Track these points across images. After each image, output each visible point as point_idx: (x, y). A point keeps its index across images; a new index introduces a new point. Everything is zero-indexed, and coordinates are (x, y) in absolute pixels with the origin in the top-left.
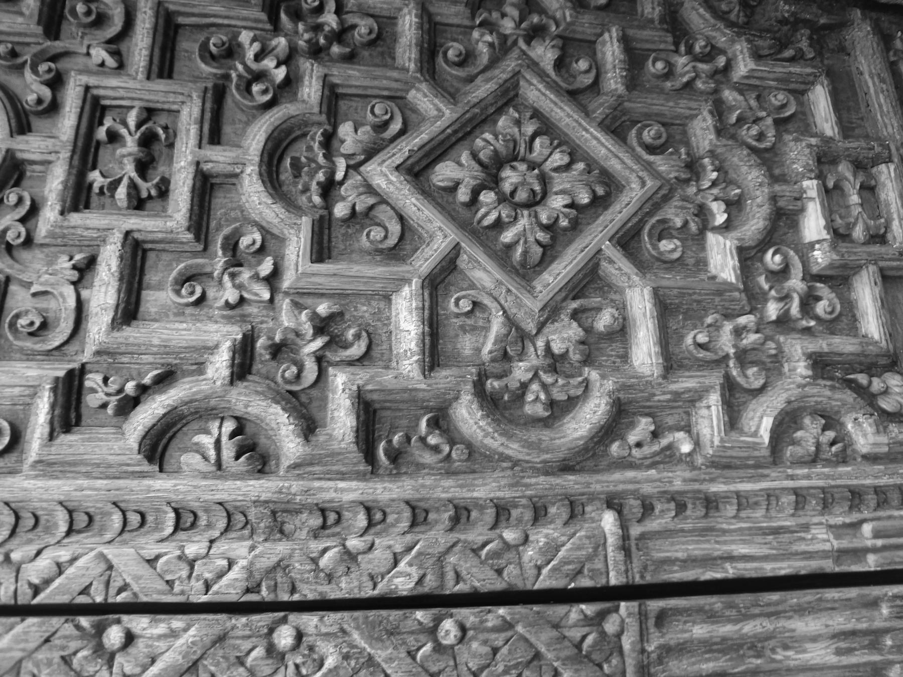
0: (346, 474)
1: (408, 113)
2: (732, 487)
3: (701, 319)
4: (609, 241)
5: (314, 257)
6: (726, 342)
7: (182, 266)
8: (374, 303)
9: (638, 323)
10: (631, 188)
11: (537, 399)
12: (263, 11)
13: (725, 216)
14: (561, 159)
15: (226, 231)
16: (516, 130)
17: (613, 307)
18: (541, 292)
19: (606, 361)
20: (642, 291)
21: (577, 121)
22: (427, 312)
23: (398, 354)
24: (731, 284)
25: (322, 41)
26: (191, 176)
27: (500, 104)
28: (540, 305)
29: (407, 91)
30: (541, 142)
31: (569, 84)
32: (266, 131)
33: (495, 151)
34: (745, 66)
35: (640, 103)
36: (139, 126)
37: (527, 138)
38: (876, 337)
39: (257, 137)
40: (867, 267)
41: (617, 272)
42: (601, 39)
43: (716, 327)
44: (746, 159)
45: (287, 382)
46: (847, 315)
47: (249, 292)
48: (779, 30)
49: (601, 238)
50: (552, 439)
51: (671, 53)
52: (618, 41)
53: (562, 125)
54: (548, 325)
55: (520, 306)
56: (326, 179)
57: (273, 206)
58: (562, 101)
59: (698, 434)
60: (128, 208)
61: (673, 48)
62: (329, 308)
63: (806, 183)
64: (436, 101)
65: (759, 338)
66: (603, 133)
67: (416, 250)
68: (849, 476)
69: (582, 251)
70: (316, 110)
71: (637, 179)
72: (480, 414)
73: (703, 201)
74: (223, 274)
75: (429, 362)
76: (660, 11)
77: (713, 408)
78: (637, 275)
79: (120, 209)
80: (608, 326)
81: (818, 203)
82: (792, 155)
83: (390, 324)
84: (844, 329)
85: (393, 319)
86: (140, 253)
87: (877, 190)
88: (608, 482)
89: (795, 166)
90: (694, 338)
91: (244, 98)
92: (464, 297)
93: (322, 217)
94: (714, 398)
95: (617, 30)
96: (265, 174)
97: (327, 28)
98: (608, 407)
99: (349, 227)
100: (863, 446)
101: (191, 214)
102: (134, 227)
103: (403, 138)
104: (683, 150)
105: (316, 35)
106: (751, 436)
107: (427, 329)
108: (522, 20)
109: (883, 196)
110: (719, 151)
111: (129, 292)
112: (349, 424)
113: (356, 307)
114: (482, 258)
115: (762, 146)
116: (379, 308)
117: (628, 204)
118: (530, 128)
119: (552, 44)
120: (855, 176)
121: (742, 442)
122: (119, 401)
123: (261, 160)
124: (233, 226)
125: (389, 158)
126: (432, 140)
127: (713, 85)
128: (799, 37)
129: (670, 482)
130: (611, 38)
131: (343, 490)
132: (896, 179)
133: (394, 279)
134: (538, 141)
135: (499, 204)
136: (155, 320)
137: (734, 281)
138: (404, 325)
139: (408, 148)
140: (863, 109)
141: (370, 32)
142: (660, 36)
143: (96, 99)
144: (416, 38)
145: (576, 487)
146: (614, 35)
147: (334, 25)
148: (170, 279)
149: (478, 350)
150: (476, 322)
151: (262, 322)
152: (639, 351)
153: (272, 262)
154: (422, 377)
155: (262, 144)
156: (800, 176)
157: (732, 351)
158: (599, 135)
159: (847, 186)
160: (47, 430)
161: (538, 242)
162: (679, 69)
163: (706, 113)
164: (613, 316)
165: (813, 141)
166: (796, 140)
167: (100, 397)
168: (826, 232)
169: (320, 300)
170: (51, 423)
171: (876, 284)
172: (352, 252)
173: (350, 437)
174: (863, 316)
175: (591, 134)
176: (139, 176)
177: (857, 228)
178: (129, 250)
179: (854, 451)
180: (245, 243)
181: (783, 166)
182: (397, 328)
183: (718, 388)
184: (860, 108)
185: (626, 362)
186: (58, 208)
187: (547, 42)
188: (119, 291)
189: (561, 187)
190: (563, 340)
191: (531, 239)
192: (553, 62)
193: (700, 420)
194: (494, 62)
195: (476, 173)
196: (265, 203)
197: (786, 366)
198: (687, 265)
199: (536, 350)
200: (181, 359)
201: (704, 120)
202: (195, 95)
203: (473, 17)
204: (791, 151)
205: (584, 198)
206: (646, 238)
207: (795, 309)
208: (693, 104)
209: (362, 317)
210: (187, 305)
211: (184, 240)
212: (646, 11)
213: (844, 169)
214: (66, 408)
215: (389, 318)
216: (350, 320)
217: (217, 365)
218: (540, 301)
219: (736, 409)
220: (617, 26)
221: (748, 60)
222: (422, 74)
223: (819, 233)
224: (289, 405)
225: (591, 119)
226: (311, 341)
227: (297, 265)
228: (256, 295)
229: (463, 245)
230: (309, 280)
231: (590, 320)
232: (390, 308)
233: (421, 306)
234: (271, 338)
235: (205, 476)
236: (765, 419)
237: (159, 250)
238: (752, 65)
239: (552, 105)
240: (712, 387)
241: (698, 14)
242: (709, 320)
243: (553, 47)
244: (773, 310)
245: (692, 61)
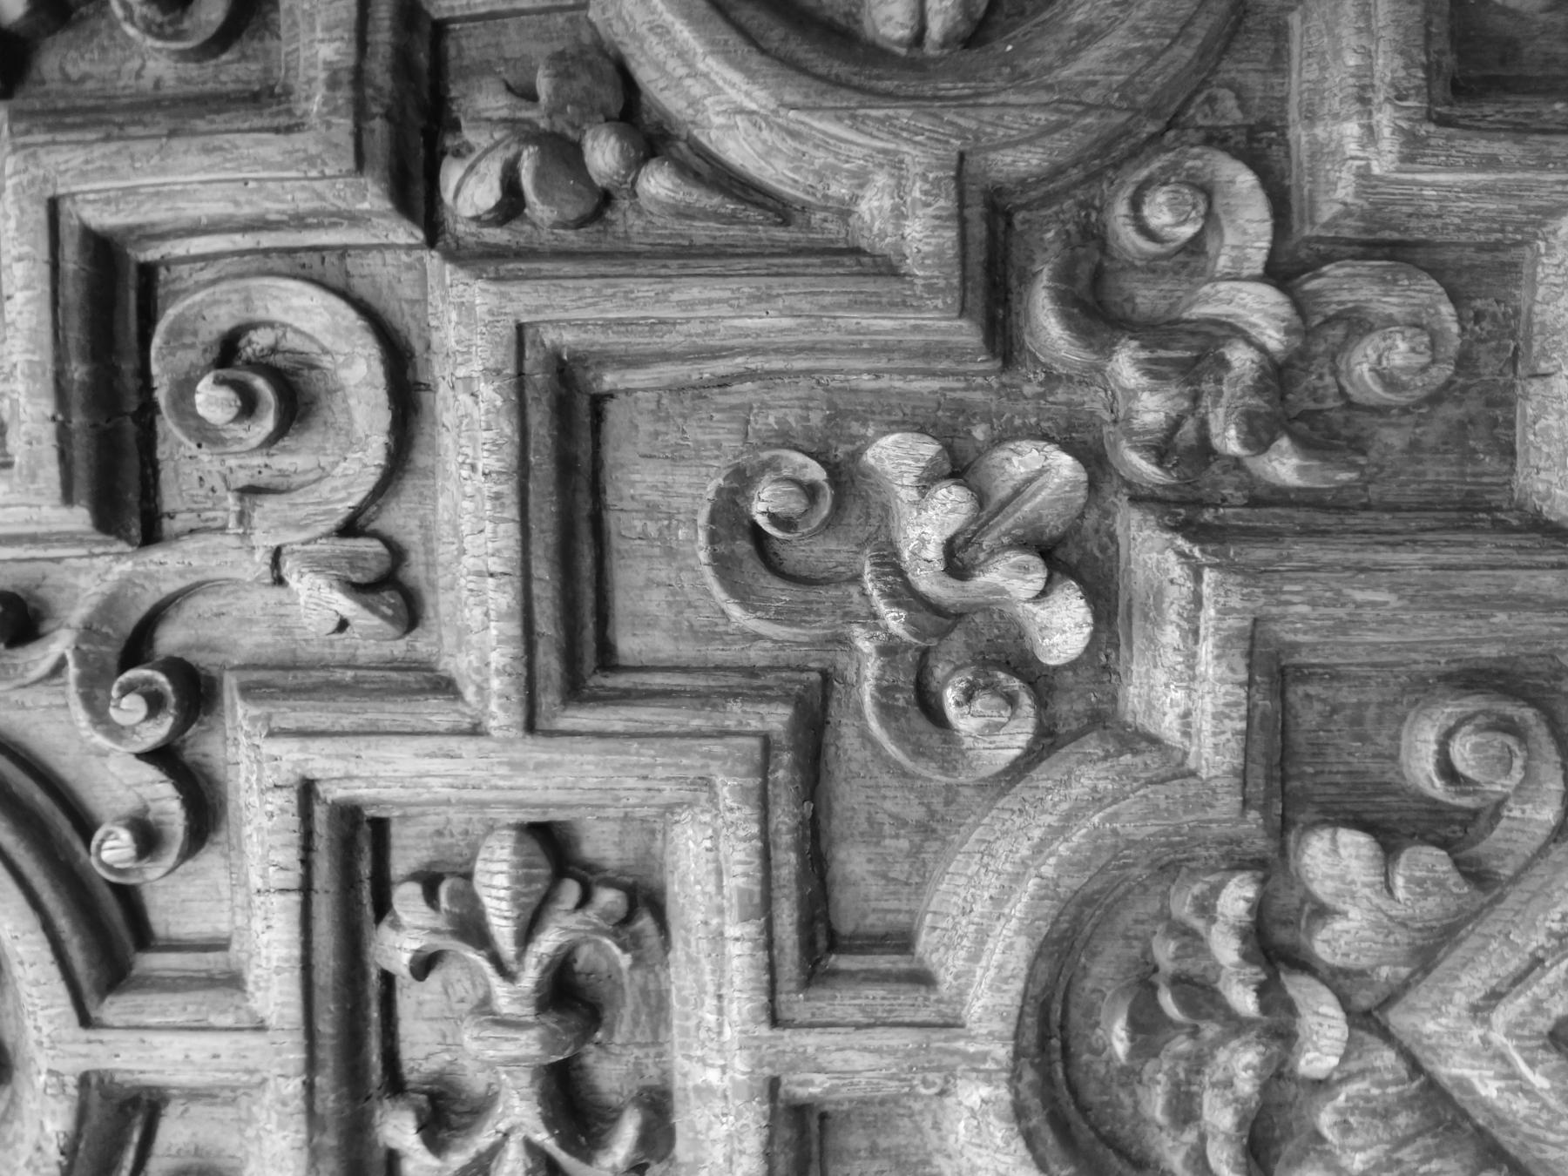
12: (963, 312)
25: (1230, 441)
26: (753, 1142)
32: (1026, 929)
36: (527, 933)
70: (1228, 803)
91: (918, 752)
97: (1241, 357)
105: (1196, 398)
125: (1520, 979)
143: (349, 816)
147: (1274, 339)
176: (564, 1145)
202: (726, 788)
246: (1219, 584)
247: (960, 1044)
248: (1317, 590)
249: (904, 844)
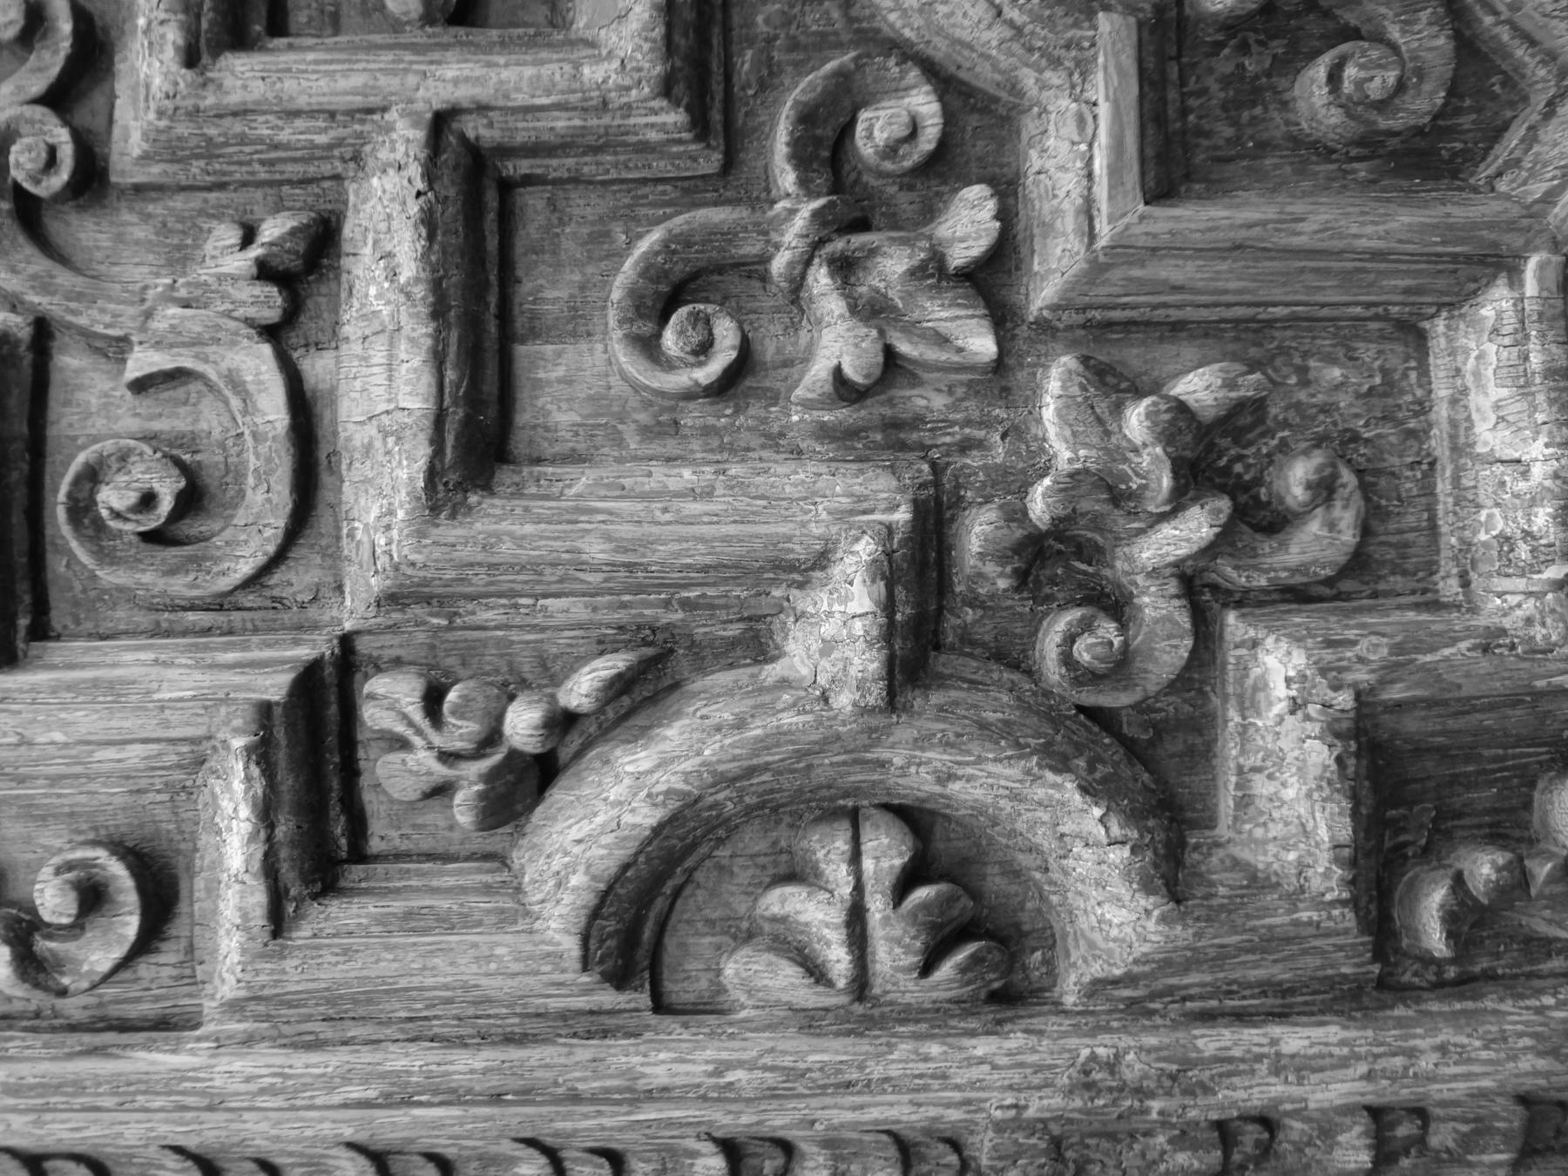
0: (1291, 991)
7: (655, 236)
8: (1367, 351)
15: (800, 90)
23: (1467, 545)
45: (1081, 676)
47: (911, 329)
60: (428, 19)
62: (1230, 384)
67: (1497, 133)
74: (808, 263)
79: (396, 26)
85: (1442, 412)
86: (491, 199)
99: (1244, 48)
101: (669, 26)
102: (463, 94)
111: (472, 356)
112: (1323, 834)
113: (1303, 371)
116: (1384, 372)
122: (491, 777)
124: (830, 66)
131: (1303, 1067)
133: (1455, 257)
136: (574, 458)
148: (616, 295)
151: (965, 447)
153: (991, 205)
160: (258, 898)
167: (423, 762)
169: (1169, 349)
170: (270, 870)
172: (1264, 147)
178: (452, 192)
180: (881, 137)
182: (1461, 448)
186: (173, 36)
188: (438, 359)
200: (686, 604)
209: (1325, 409)
210: (689, 395)
211: (653, 136)
214: (313, 811)
216: (1286, 424)
217: (828, 629)
226: (1163, 517)
227: (1088, 210)
228: (942, 340)
230: (1136, 272)
232: (1424, 371)
235: (809, 1022)
237: (556, 182)
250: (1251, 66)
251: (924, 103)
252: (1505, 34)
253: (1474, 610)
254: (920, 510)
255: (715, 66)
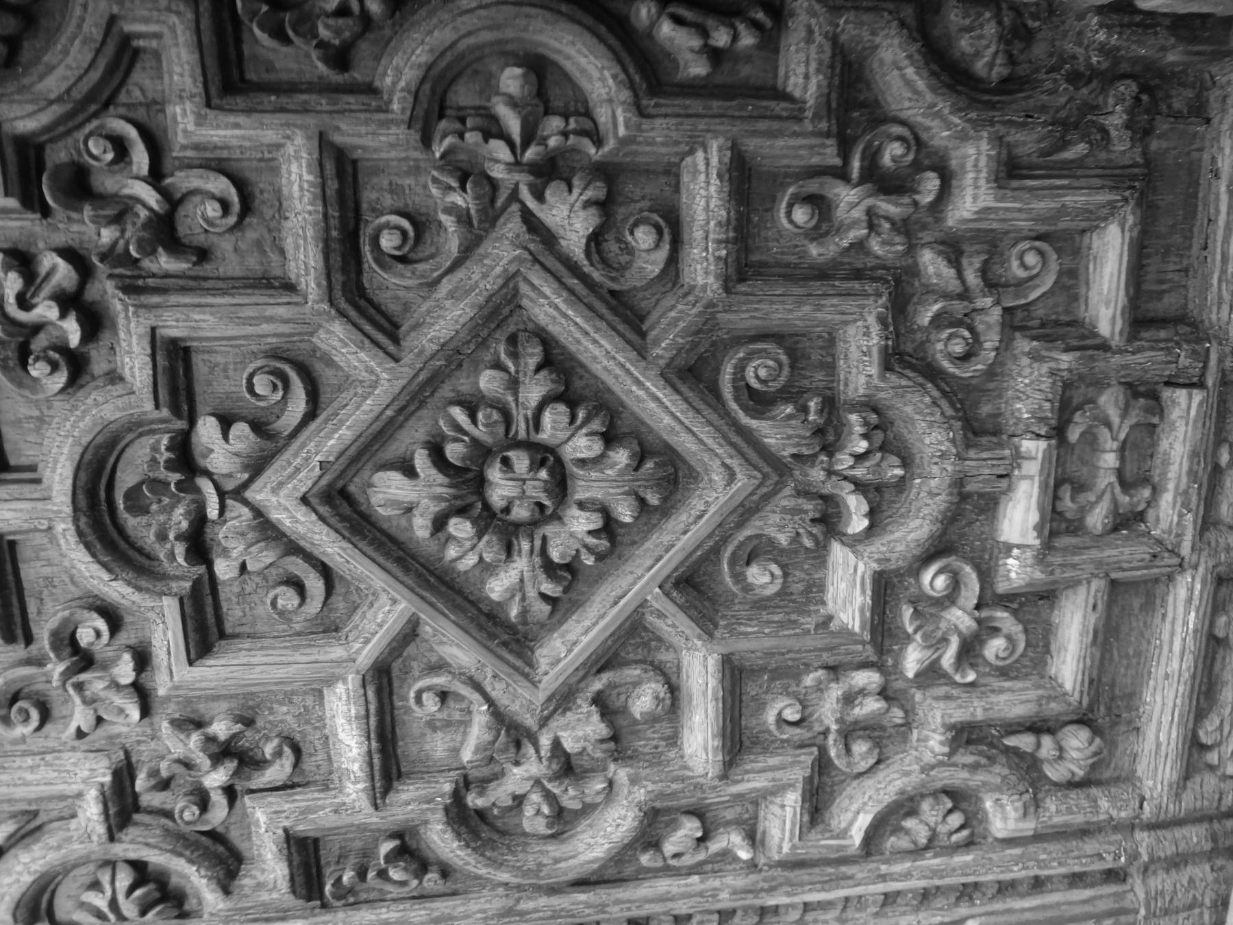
0: (289, 910)
1: (319, 368)
2: (797, 899)
3: (797, 677)
4: (660, 587)
5: (193, 656)
6: (828, 711)
9: (695, 702)
10: (710, 480)
11: (538, 812)
13: (866, 523)
14: (589, 448)
16: (510, 399)
17: (658, 682)
18: (546, 673)
19: (645, 746)
20: (705, 658)
21: (622, 366)
22: (373, 721)
23: (340, 768)
24: (851, 633)
27: (484, 333)
28: (542, 696)
29: (312, 334)
30: (554, 421)
31: (613, 279)
32: (70, 459)
33: (475, 442)
34: (975, 198)
35: (747, 311)
37: (529, 413)
38: (1068, 686)
39: (59, 471)
40: (1089, 583)
41: (670, 629)
42: (689, 160)
43: (819, 688)
44: (928, 411)
46: (1037, 646)
48: (1071, 99)
49: (647, 583)
50: (557, 861)
51: (829, 180)
52: (720, 176)
53: (596, 368)
54: (556, 716)
55: (515, 696)
56: (191, 523)
57: (114, 584)
58: (597, 330)
59: (764, 833)
61: (837, 161)
63: (1028, 445)
64: (363, 355)
65: (879, 709)
66: (668, 390)
68: (964, 869)
69: (616, 603)
70: (149, 406)
71: (722, 470)
72: (456, 844)
73: (835, 491)
75: (382, 786)
76: (819, 86)
77: (788, 809)
78: (699, 638)
80: (647, 713)
81: (1036, 485)
82: (1022, 382)
83: (324, 726)
84: (1025, 666)
85: (328, 721)
87: (1158, 430)
88: (629, 901)
89: (1018, 406)
90: (780, 714)
92: (429, 689)
93: (197, 584)
94: (793, 798)
95: (720, 149)
96: (87, 530)
98: (636, 823)
100: (999, 830)
103: (313, 426)
104: (813, 405)
105: (123, 231)
106: (837, 837)
107: (374, 744)
108: (529, 136)
109: (1164, 445)
110: (882, 395)
113: (271, 709)
114: (452, 632)
115: (965, 372)
117: (700, 517)
118: (533, 393)
119: (584, 198)
120: (1124, 415)
121: (823, 846)
123: (76, 509)
125: (291, 477)
126: (360, 436)
127: (900, 248)
128: (1111, 101)
129: (714, 896)
130: (707, 165)
132: (1195, 421)
134: (547, 418)
135: (480, 539)
137: (857, 629)
138: (342, 736)
139: (319, 458)
140: (1195, 249)
141: (225, 205)
142: (812, 147)
144: (315, 224)
145: (587, 911)
146: (714, 161)
149: (456, 751)
150: (449, 715)
151: (139, 742)
152: (692, 738)
154: (371, 810)
155: (69, 482)
156: (1022, 427)
157: (834, 727)
158: (660, 395)
159: (1104, 433)
161: (544, 597)
162: (841, 213)
163: (871, 320)
164: (657, 698)
165: (1066, 360)
166: (1036, 357)
168: (1035, 534)
169: (216, 704)
171: (1094, 607)
173: (284, 885)
174: (1059, 652)
175: (647, 390)
177: (1097, 510)
179: (986, 829)
181: (1000, 396)
183: (800, 786)
184: (1190, 247)
185: (675, 744)
187: (576, 191)
189: (587, 495)
190: (577, 739)
191: (532, 593)
192: (584, 241)
193: (770, 816)
194: (468, 251)
195: (440, 490)
196: (100, 578)
197: (915, 732)
198: (792, 594)
199: (537, 751)
201: (867, 334)
203: (426, 142)
204: (1019, 374)
205: (625, 513)
206: (726, 566)
207: (948, 659)
208: (850, 305)
209: (281, 721)
212: (792, 80)
213: (1110, 402)
215: (321, 719)
216: (265, 728)
218: (544, 690)
219: (828, 789)
220: (721, 140)
221: (982, 182)
222: (331, 302)
223: (1023, 535)
224: (196, 854)
225: (649, 363)
228: (121, 711)
229: (422, 616)
231: (623, 697)
232: (322, 704)
233: (363, 712)
234: (154, 773)
236: (861, 816)
238: (987, 199)
239: (578, 335)
240: (790, 785)
241: (903, 76)
242: (809, 680)
243: (587, 204)
244: (913, 659)
245: (869, 196)
246: (134, 313)
247: (49, 507)
248: (179, 315)
249: (32, 426)
250: (248, 589)
251: (102, 625)
252: (348, 577)
253: (341, 792)
254: (116, 774)
255: (16, 611)
